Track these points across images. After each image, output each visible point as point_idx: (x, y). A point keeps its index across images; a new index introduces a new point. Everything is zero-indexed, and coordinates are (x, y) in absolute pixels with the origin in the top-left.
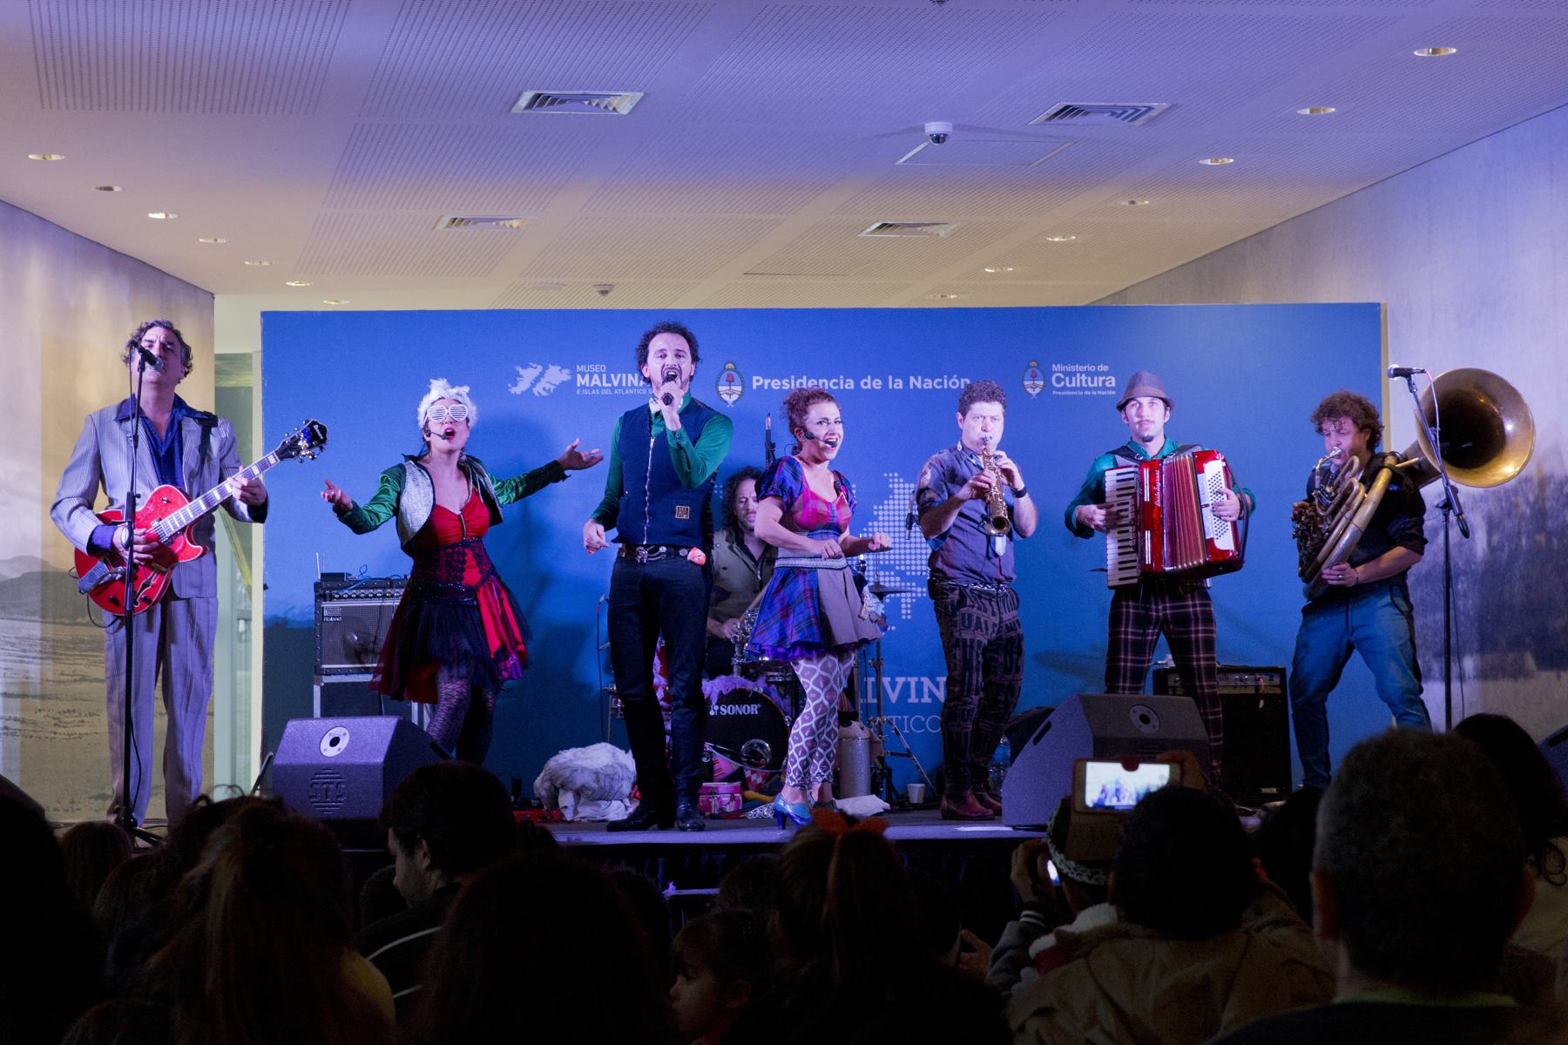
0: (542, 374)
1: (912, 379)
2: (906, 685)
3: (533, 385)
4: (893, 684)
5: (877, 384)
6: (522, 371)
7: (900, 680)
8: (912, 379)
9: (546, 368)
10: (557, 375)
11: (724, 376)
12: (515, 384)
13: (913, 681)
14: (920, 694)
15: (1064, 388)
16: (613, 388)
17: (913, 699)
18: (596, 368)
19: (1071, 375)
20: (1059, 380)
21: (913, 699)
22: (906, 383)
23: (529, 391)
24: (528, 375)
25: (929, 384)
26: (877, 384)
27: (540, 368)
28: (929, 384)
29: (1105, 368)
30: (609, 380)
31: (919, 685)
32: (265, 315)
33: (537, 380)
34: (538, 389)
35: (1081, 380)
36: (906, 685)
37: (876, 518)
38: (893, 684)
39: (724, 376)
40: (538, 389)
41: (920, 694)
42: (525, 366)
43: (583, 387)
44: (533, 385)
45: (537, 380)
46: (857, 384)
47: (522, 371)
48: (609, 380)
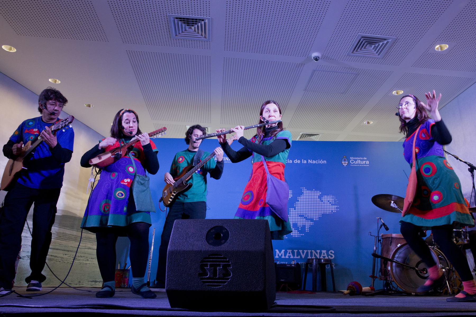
1: (309, 160)
2: (307, 253)
4: (303, 252)
5: (299, 162)
7: (305, 251)
8: (309, 160)
13: (309, 251)
14: (311, 256)
15: (354, 164)
20: (352, 162)
22: (307, 161)
25: (314, 162)
26: (299, 162)
29: (366, 159)
31: (311, 253)
35: (359, 162)
36: (307, 253)
37: (298, 201)
38: (303, 252)
46: (293, 161)
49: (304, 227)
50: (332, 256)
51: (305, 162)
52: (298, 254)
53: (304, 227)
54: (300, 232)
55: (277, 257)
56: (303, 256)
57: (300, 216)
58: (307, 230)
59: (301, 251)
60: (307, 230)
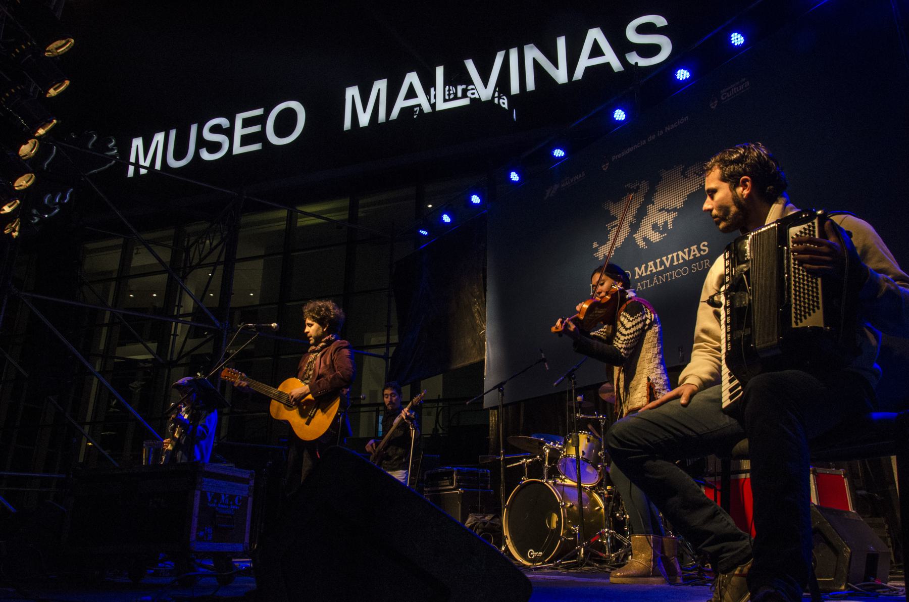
2: (673, 257)
4: (667, 259)
5: (654, 137)
13: (675, 255)
14: (678, 260)
17: (676, 263)
21: (676, 263)
36: (673, 257)
38: (667, 259)
41: (678, 260)
49: (666, 223)
50: (704, 251)
52: (662, 263)
53: (666, 223)
54: (661, 233)
55: (637, 277)
56: (668, 265)
57: (660, 211)
58: (670, 226)
59: (664, 259)
60: (670, 226)
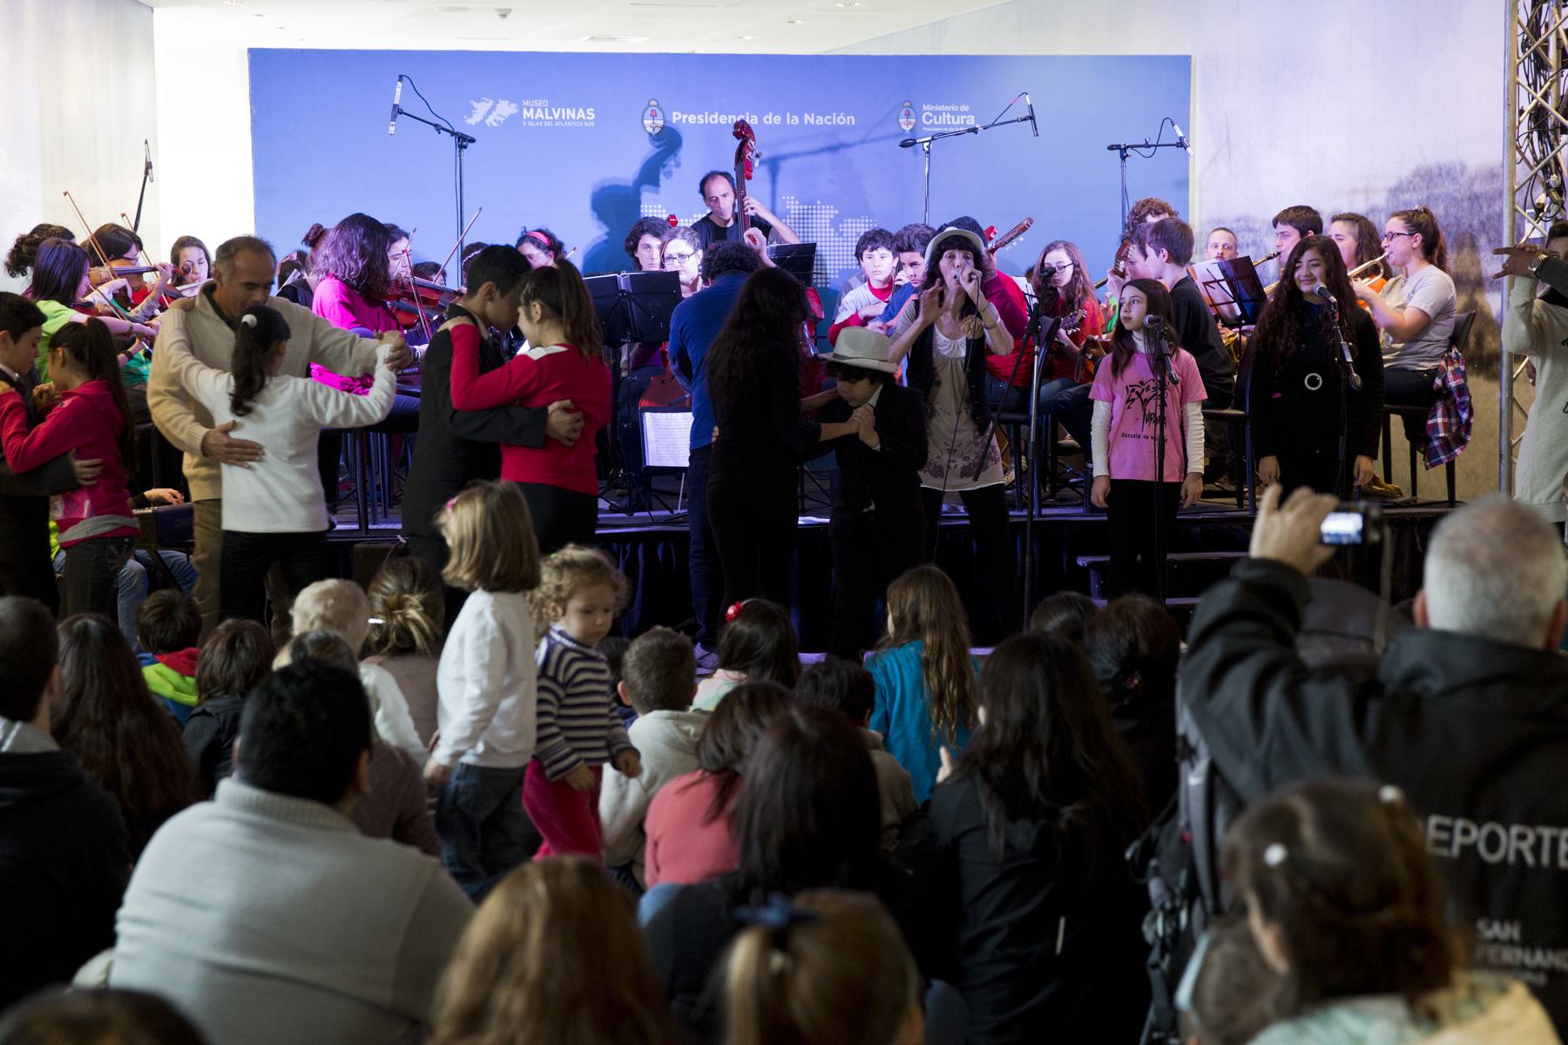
0: (493, 108)
3: (486, 117)
5: (777, 120)
6: (476, 105)
9: (496, 102)
10: (505, 109)
11: (649, 112)
12: (470, 116)
15: (933, 125)
16: (554, 121)
18: (540, 103)
19: (938, 113)
20: (928, 118)
22: (801, 119)
23: (482, 122)
24: (481, 108)
25: (820, 120)
26: (777, 120)
27: (491, 102)
28: (820, 120)
29: (966, 108)
30: (551, 114)
32: (251, 51)
33: (489, 112)
34: (490, 121)
39: (649, 112)
40: (490, 121)
42: (479, 101)
43: (528, 119)
44: (486, 117)
45: (489, 112)
47: (476, 105)
48: (551, 114)
51: (796, 120)
